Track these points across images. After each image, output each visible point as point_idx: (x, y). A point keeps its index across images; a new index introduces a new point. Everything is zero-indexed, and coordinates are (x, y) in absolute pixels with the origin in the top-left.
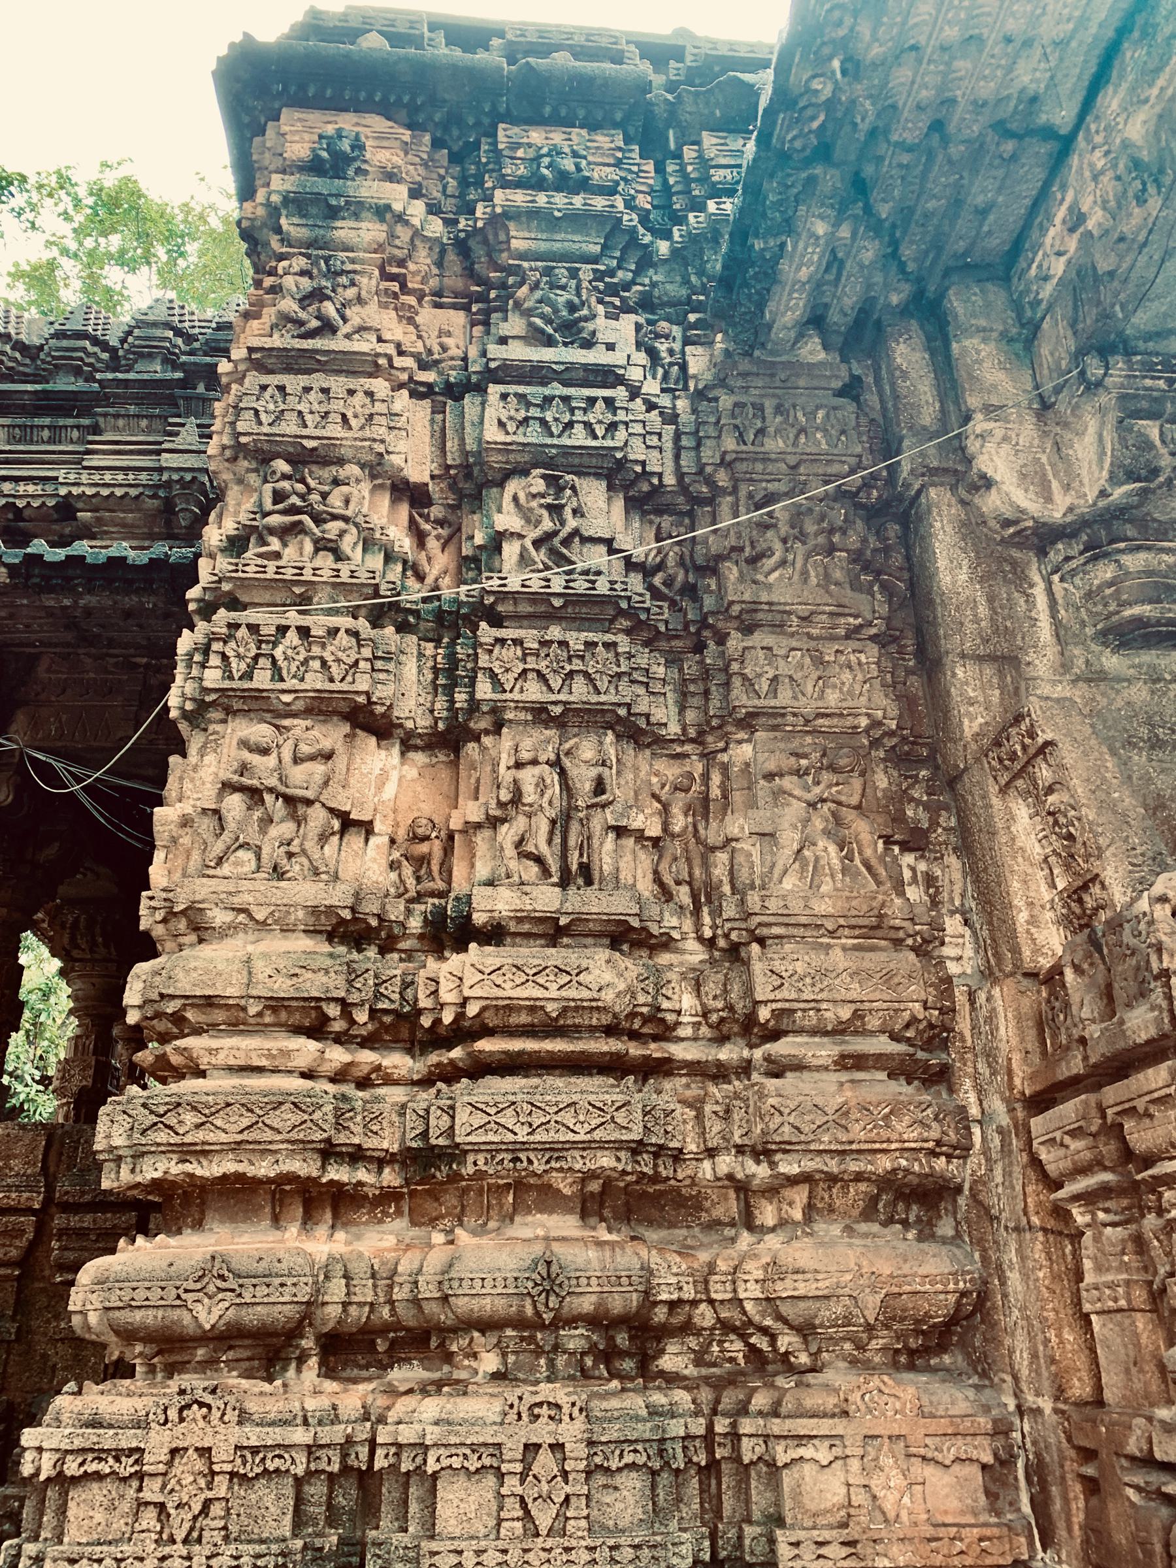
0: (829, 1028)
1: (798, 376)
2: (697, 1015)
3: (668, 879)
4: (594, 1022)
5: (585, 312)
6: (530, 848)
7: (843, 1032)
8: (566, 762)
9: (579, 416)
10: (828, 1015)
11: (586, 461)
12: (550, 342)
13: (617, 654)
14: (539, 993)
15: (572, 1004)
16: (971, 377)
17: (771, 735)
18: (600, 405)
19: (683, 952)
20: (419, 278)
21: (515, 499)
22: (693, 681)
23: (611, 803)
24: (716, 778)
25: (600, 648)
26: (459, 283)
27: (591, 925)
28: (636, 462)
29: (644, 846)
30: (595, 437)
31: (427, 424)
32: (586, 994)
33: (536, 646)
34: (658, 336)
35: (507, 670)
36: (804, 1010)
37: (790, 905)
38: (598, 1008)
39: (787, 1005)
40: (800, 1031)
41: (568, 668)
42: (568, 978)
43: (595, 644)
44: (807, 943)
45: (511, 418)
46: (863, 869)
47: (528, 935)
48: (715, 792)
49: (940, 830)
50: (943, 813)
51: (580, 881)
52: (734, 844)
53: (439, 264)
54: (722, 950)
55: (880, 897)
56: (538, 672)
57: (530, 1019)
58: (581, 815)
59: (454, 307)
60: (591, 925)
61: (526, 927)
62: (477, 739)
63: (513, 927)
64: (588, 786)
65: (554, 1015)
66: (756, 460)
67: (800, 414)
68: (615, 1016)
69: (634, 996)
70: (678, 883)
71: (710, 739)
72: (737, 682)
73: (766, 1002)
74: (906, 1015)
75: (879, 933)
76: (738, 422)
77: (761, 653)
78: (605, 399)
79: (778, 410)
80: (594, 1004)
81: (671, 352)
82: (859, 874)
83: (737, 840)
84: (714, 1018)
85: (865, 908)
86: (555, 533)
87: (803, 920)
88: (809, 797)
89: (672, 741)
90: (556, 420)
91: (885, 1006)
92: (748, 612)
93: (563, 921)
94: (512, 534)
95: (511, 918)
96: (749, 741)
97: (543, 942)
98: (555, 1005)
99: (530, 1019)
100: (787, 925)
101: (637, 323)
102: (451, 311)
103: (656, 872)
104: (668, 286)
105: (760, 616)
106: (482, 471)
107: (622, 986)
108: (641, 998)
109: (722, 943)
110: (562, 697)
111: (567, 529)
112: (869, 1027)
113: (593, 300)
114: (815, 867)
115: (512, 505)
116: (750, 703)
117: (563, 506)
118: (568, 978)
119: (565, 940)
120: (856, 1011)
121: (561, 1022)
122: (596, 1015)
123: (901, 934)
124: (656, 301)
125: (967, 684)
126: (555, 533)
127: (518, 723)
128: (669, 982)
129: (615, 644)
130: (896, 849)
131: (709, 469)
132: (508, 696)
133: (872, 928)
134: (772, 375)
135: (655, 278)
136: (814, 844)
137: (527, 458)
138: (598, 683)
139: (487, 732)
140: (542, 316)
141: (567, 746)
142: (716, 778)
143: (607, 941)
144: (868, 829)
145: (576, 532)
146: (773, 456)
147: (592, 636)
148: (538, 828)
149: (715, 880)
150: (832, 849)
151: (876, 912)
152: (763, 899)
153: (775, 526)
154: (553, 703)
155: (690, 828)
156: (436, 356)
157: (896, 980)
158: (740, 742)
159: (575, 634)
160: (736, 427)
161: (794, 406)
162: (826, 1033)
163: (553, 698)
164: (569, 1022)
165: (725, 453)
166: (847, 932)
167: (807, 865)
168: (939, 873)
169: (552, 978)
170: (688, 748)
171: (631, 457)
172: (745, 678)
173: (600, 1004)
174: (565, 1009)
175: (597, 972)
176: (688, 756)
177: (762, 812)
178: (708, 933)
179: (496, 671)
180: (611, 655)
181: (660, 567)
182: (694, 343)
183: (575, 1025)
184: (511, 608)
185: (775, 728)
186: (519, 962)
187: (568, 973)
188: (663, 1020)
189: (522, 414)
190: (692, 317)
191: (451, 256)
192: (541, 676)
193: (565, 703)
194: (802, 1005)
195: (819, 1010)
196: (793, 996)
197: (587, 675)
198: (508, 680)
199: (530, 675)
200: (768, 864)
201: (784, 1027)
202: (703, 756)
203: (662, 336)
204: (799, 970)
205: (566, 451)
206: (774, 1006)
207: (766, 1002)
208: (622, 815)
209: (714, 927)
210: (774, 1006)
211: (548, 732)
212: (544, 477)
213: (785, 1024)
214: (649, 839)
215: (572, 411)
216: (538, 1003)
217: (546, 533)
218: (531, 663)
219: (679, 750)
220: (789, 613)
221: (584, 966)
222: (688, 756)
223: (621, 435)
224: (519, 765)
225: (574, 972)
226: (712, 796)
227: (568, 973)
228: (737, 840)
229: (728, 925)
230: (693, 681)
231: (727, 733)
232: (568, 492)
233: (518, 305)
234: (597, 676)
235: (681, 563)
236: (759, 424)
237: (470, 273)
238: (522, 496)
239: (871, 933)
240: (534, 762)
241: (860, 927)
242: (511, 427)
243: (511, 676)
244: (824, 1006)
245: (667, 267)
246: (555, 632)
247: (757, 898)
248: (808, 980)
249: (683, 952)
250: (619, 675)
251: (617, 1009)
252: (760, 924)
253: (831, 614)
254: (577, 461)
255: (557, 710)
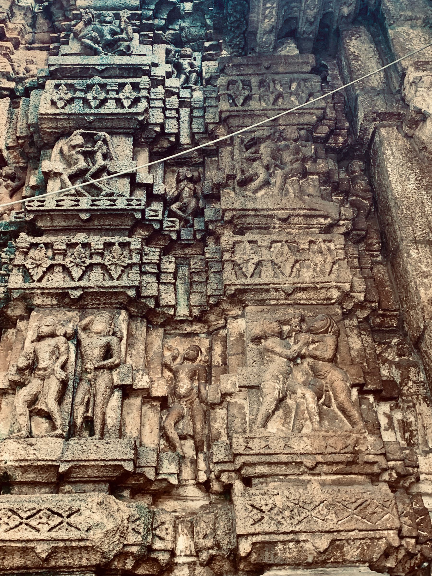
0: (310, 560)
1: (277, 64)
2: (191, 555)
3: (173, 434)
4: (84, 562)
5: (124, 35)
6: (40, 405)
7: (324, 563)
8: (82, 335)
9: (112, 95)
10: (308, 546)
11: (116, 123)
12: (96, 53)
13: (131, 251)
14: (30, 535)
15: (62, 544)
16: (403, 49)
17: (260, 308)
18: (128, 88)
19: (184, 498)
20: (16, 33)
21: (61, 151)
22: (198, 273)
23: (118, 365)
24: (218, 349)
25: (117, 246)
26: (46, 37)
27: (89, 471)
28: (156, 124)
29: (153, 406)
30: (123, 107)
31: (6, 113)
32: (74, 534)
33: (64, 247)
34: (183, 56)
35: (38, 266)
36: (284, 542)
37: (271, 445)
38: (86, 548)
39: (267, 538)
40: (282, 565)
41: (88, 262)
42: (60, 520)
43: (113, 244)
44: (290, 481)
45: (61, 99)
46: (340, 413)
47: (33, 484)
48: (217, 360)
49: (410, 384)
50: (412, 369)
51: (86, 434)
52: (228, 399)
53: (33, 25)
54: (216, 493)
55: (354, 436)
56: (63, 266)
57: (23, 561)
58: (90, 376)
59: (41, 49)
60: (89, 471)
61: (30, 476)
62: (14, 326)
63: (18, 476)
64: (97, 352)
65: (44, 556)
66: (245, 116)
67: (278, 87)
68: (103, 555)
69: (123, 535)
70: (183, 437)
71: (212, 317)
72: (228, 267)
73: (246, 536)
74: (383, 543)
75: (355, 469)
76: (231, 92)
77: (248, 246)
78: (132, 84)
79: (261, 84)
80: (82, 544)
81: (192, 65)
82: (336, 417)
83: (230, 394)
84: (204, 556)
85: (340, 445)
86: (87, 170)
87: (284, 458)
88: (288, 352)
89: (182, 322)
90: (95, 98)
91: (361, 535)
92: (238, 218)
93: (63, 468)
94: (55, 174)
95: (16, 468)
96: (243, 316)
97: (47, 490)
98: (46, 546)
99: (23, 561)
100: (270, 464)
101: (167, 49)
102: (38, 52)
103: (162, 429)
104: (191, 29)
105: (249, 220)
106: (40, 137)
107: (110, 525)
108: (132, 538)
109: (216, 486)
110: (81, 284)
111: (97, 166)
112: (348, 557)
113: (130, 29)
114: (296, 413)
115: (59, 156)
116: (238, 282)
117: (95, 152)
118: (60, 520)
119: (67, 487)
120: (333, 541)
121: (53, 563)
122: (85, 555)
123: (376, 469)
124: (184, 39)
125: (420, 261)
126: (87, 170)
127: (45, 307)
128: (163, 523)
129: (128, 244)
130: (371, 398)
131: (211, 127)
132: (36, 284)
133: (349, 464)
134: (258, 65)
135: (182, 25)
136: (294, 393)
137: (71, 124)
138: (112, 272)
139: (22, 318)
140: (92, 39)
141: (84, 322)
142: (218, 349)
143: (105, 487)
144: (340, 377)
145: (103, 169)
146: (258, 112)
147: (109, 239)
148: (49, 388)
149: (214, 432)
150: (310, 395)
151: (350, 449)
152: (247, 440)
153: (259, 158)
154: (73, 288)
155: (195, 390)
156: (21, 75)
157: (370, 510)
158: (236, 318)
159: (96, 238)
160: (230, 96)
161: (274, 81)
162: (309, 566)
163: (73, 284)
164: (60, 563)
165: (221, 112)
166: (325, 468)
167: (290, 412)
168: (412, 419)
169: (44, 520)
170: (196, 327)
171: (152, 121)
172: (235, 264)
173: (88, 543)
174: (54, 551)
175: (88, 513)
176: (197, 334)
177: (249, 369)
178: (203, 477)
179: (28, 266)
180: (126, 253)
181: (178, 198)
182: (208, 60)
183: (66, 566)
184: (49, 224)
185: (262, 302)
186: (15, 507)
187: (60, 515)
188: (156, 560)
189: (70, 95)
190: (207, 44)
191: (41, 20)
192: (66, 270)
193: (83, 288)
194: (282, 538)
195: (298, 542)
196: (273, 528)
197: (103, 266)
198: (37, 273)
199: (57, 269)
200: (254, 412)
201: (266, 560)
202: (209, 334)
203: (185, 56)
204: (279, 504)
205: (101, 117)
206: (255, 539)
207: (246, 536)
208: (127, 376)
209: (209, 471)
210: (255, 539)
211: (70, 314)
212: (82, 134)
213: (267, 558)
214: (156, 398)
215: (107, 92)
216: (29, 545)
217: (80, 170)
218: (59, 260)
219: (189, 330)
220: (272, 217)
221: (75, 508)
222: (197, 334)
223: (142, 105)
224: (40, 338)
225: (65, 515)
226: (214, 363)
227: (60, 515)
228: (230, 394)
229: (218, 468)
230: (198, 273)
231: (224, 311)
232: (100, 142)
233: (76, 35)
234: (113, 267)
235: (195, 194)
236: (247, 93)
237: (54, 29)
238: (66, 149)
239: (348, 469)
240: (53, 335)
241: (338, 463)
242: (60, 104)
243: (40, 271)
244: (302, 537)
245: (191, 18)
246: (81, 237)
247: (241, 440)
248: (287, 513)
249: (184, 498)
250: (130, 266)
251: (105, 548)
252: (244, 464)
253: (305, 216)
254: (109, 124)
255: (77, 294)
